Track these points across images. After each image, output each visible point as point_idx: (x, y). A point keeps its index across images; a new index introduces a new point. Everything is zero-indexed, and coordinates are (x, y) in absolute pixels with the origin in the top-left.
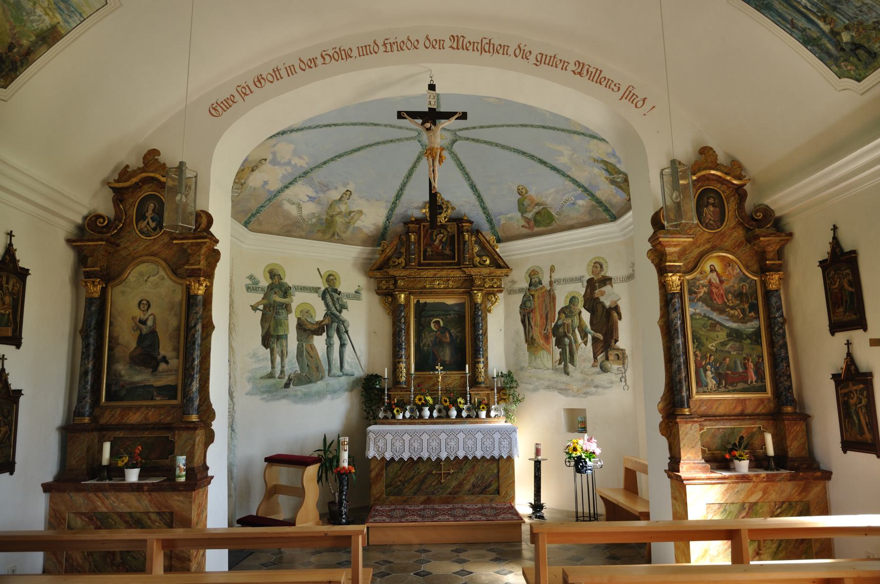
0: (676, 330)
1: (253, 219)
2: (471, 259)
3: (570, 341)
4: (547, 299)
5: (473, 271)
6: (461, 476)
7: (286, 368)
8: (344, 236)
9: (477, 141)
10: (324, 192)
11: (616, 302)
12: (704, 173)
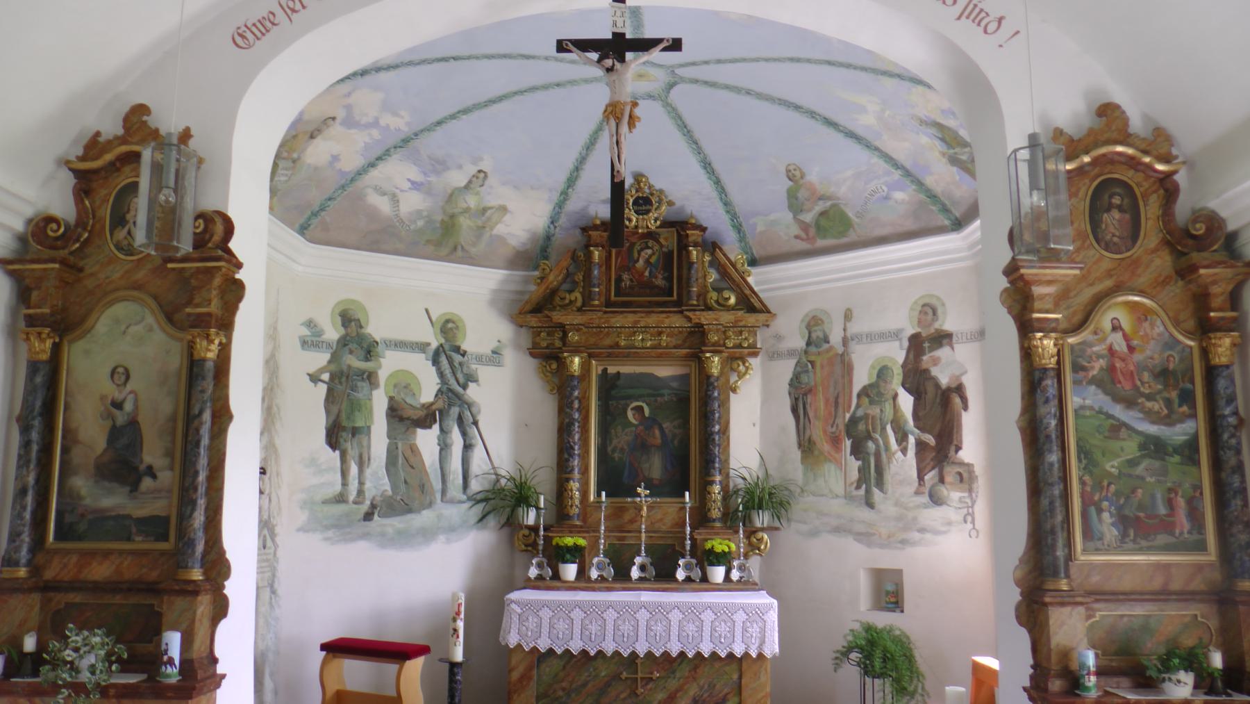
0: (1048, 437)
1: (315, 221)
2: (702, 295)
3: (878, 446)
4: (838, 369)
5: (705, 318)
6: (673, 684)
7: (368, 485)
8: (473, 250)
9: (713, 85)
10: (437, 173)
11: (958, 378)
12: (1103, 150)
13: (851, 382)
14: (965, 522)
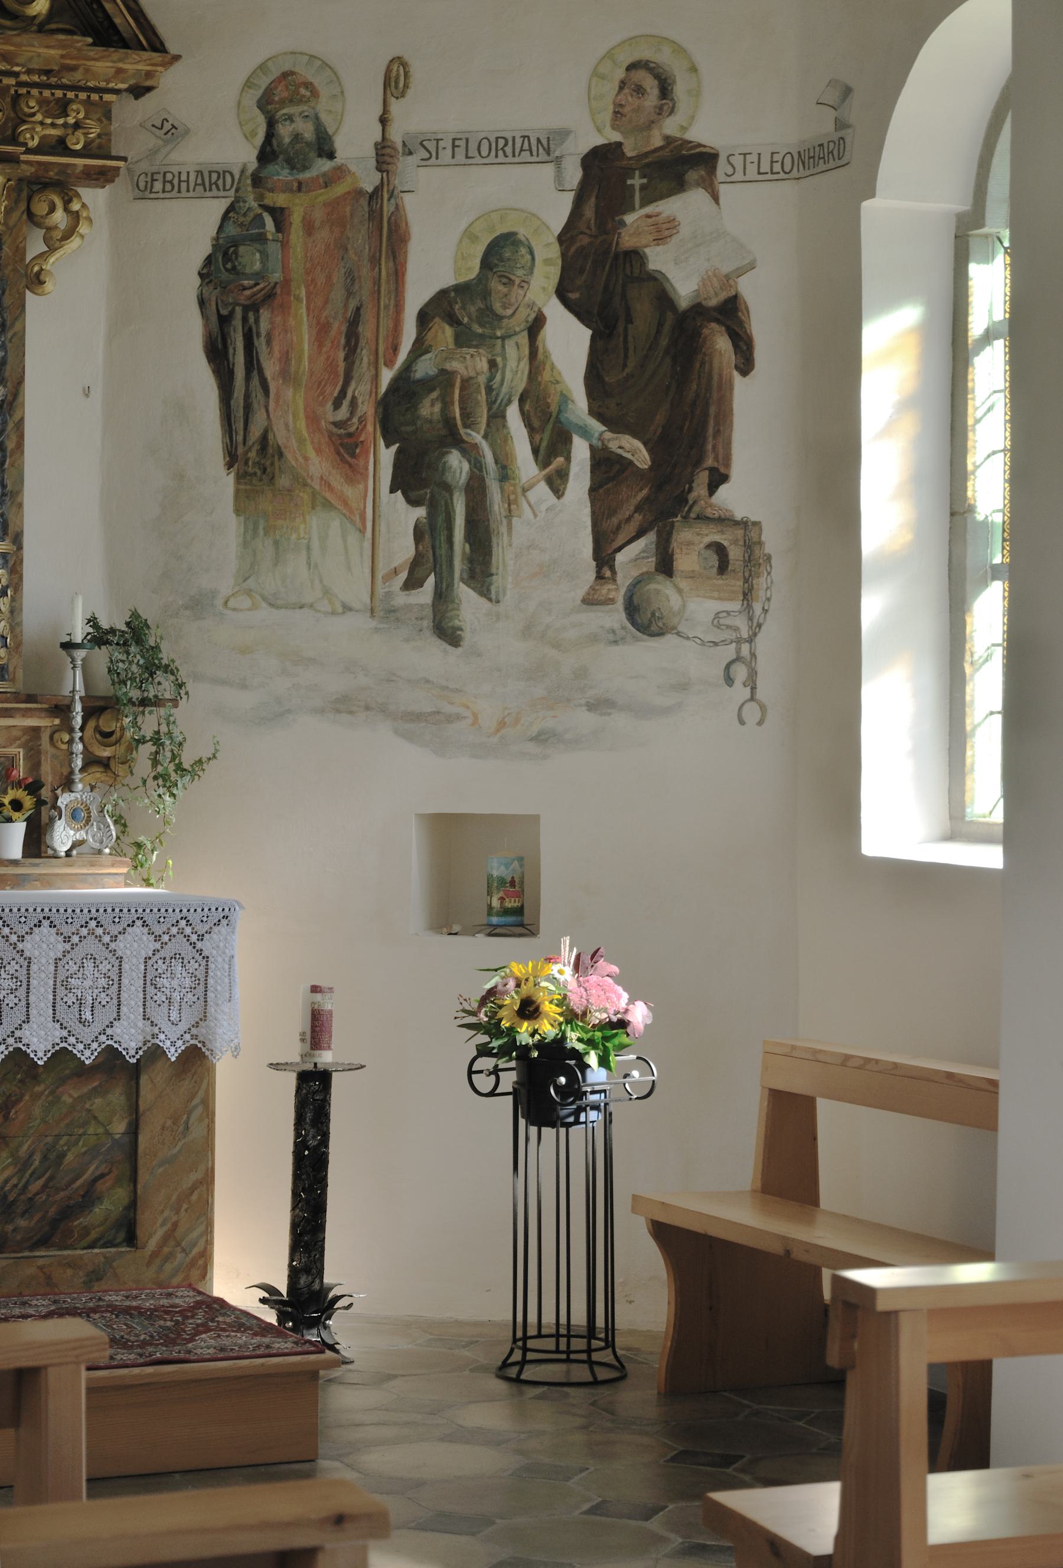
3: (477, 465)
4: (359, 238)
11: (728, 279)
13: (398, 275)
14: (729, 680)
